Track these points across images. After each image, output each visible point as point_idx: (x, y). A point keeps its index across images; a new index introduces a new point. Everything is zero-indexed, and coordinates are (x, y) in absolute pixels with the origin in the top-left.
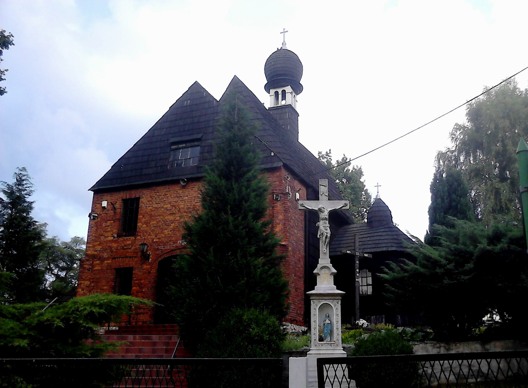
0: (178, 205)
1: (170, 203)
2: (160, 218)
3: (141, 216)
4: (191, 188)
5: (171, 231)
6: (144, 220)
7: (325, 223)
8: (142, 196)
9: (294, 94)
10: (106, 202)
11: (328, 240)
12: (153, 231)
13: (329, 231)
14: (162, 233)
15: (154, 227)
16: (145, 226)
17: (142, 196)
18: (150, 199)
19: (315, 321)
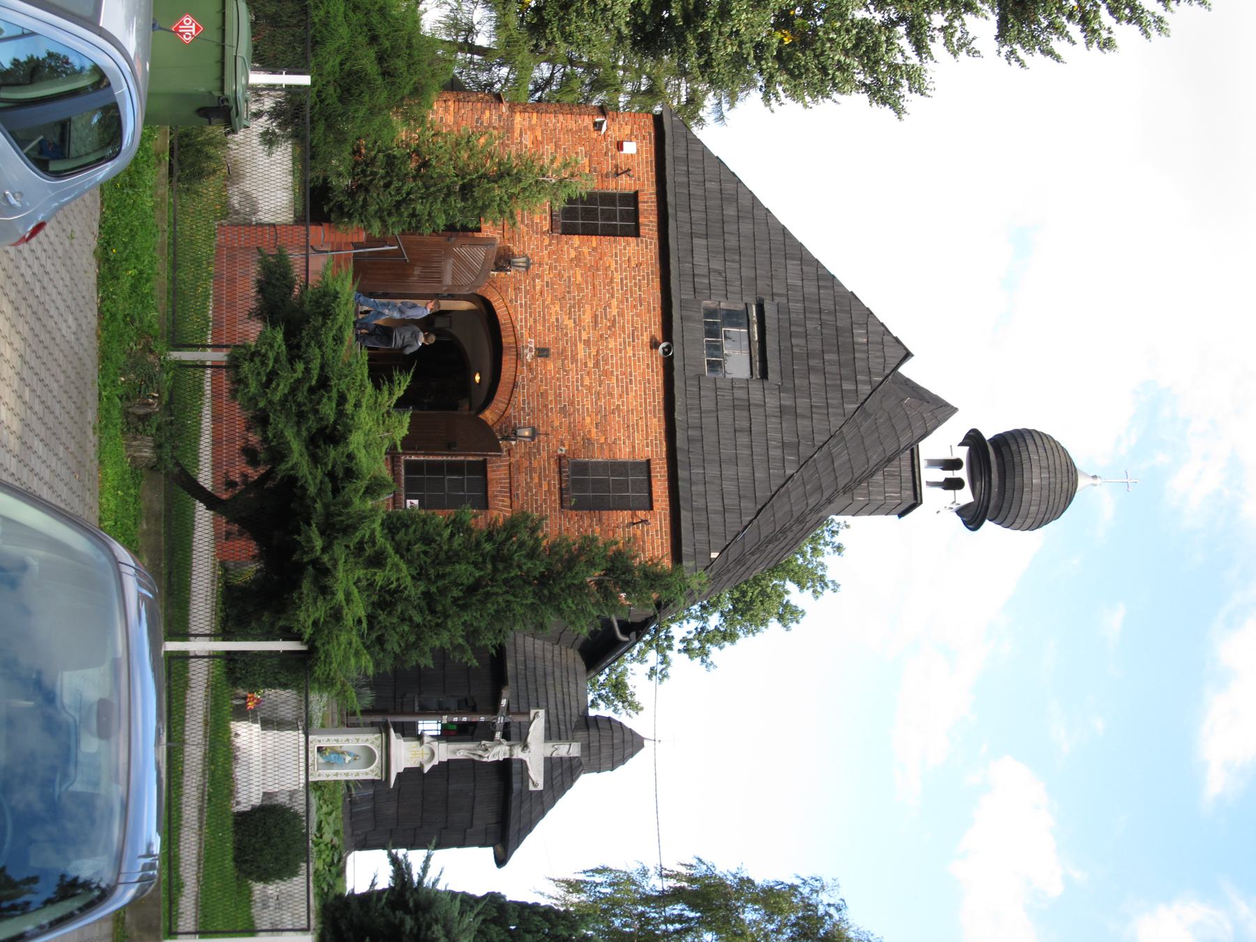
0: (614, 334)
1: (621, 314)
2: (588, 291)
3: (594, 245)
4: (652, 363)
5: (557, 319)
6: (585, 250)
7: (505, 754)
8: (642, 242)
9: (955, 507)
10: (634, 151)
11: (476, 758)
12: (560, 276)
13: (491, 759)
14: (554, 298)
15: (569, 277)
16: (573, 254)
17: (642, 242)
18: (633, 265)
19: (348, 740)
